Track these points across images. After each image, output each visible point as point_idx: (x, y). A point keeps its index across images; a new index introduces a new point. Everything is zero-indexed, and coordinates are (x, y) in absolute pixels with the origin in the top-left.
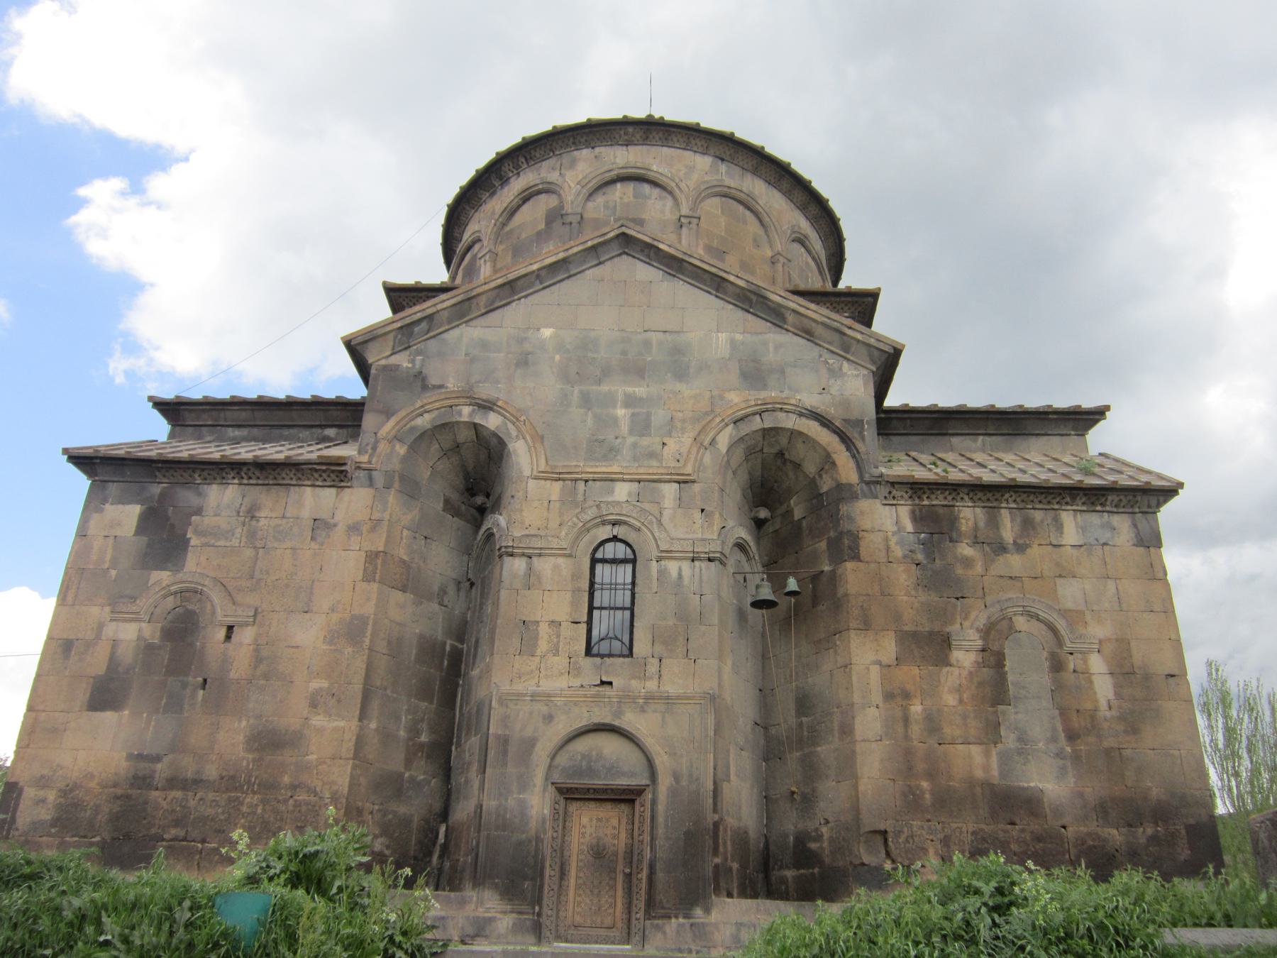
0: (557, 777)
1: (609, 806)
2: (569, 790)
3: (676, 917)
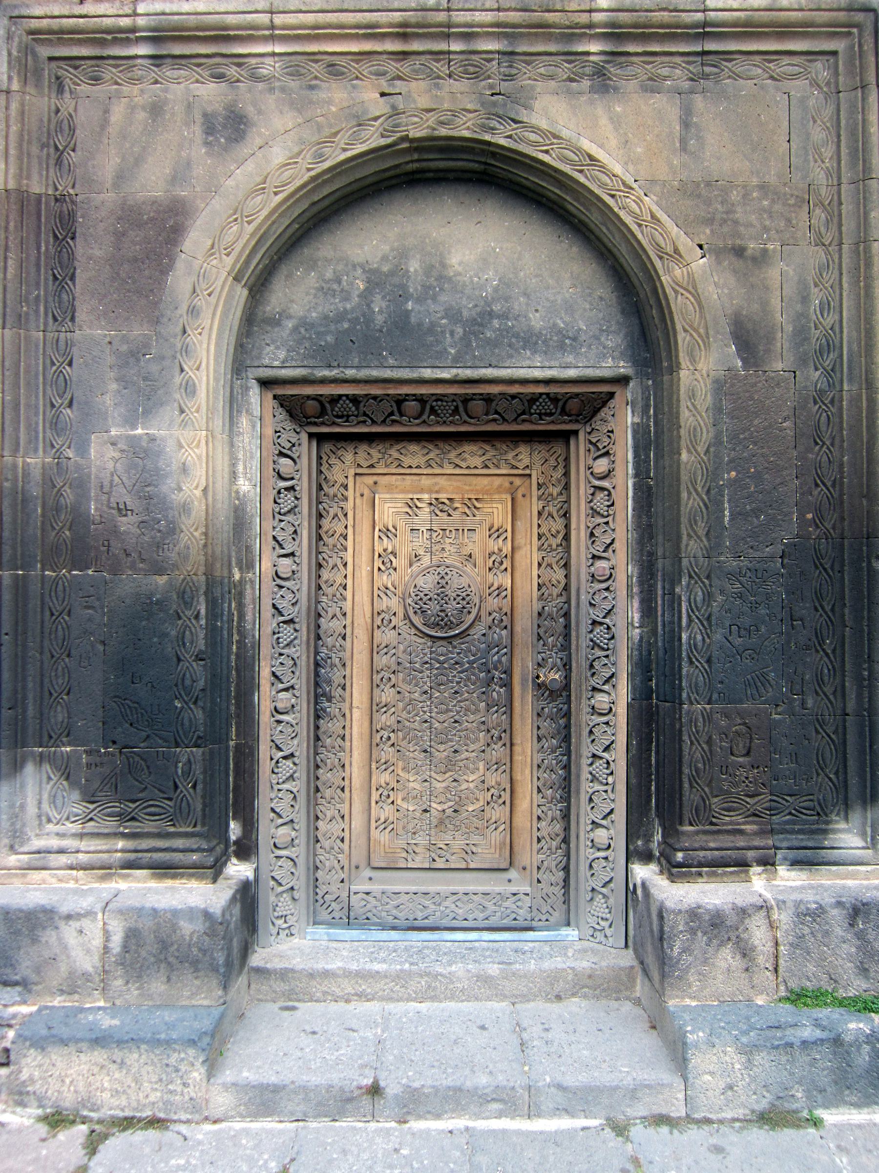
0: (276, 357)
1: (473, 455)
2: (326, 406)
3: (767, 862)
